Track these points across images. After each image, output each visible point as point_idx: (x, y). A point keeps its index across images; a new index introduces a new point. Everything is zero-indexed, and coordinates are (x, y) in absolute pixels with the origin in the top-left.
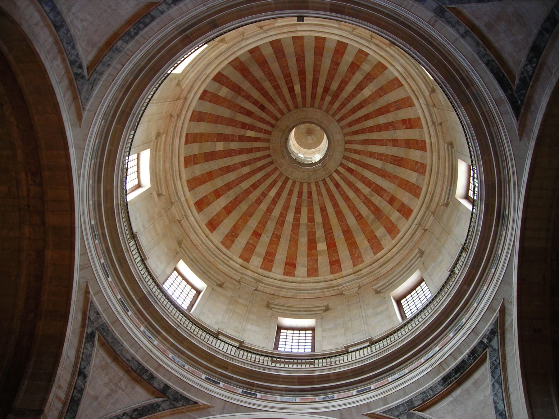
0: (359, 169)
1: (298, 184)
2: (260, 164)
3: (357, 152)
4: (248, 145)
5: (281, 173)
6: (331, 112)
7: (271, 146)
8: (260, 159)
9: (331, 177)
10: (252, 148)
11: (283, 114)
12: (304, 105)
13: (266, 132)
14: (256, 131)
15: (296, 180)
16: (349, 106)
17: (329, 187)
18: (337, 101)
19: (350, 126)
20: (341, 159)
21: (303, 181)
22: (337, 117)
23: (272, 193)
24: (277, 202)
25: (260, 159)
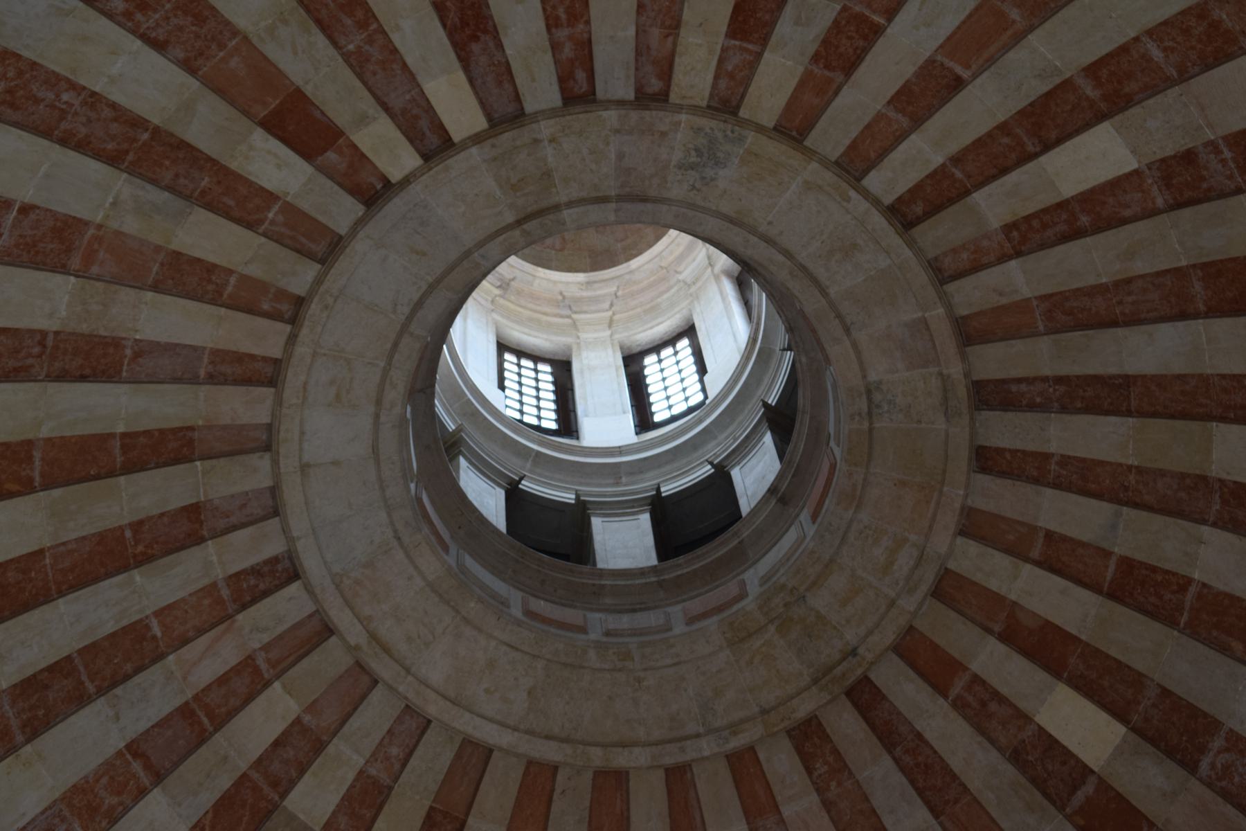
0: (207, 124)
1: (838, 127)
2: (1103, 438)
3: (188, 278)
4: (1132, 638)
5: (942, 274)
6: (328, 662)
7: (941, 541)
8: (1082, 478)
9: (506, 115)
10: (1113, 596)
11: (744, 766)
12: (538, 781)
13: (937, 668)
14: (1024, 718)
15: (829, 177)
16: (152, 698)
17: (552, 23)
18: (243, 766)
19: (193, 511)
20: (360, 245)
21: (774, 149)
22: (284, 609)
23: (1096, 156)
24: (1092, 70)
25: (1082, 478)
